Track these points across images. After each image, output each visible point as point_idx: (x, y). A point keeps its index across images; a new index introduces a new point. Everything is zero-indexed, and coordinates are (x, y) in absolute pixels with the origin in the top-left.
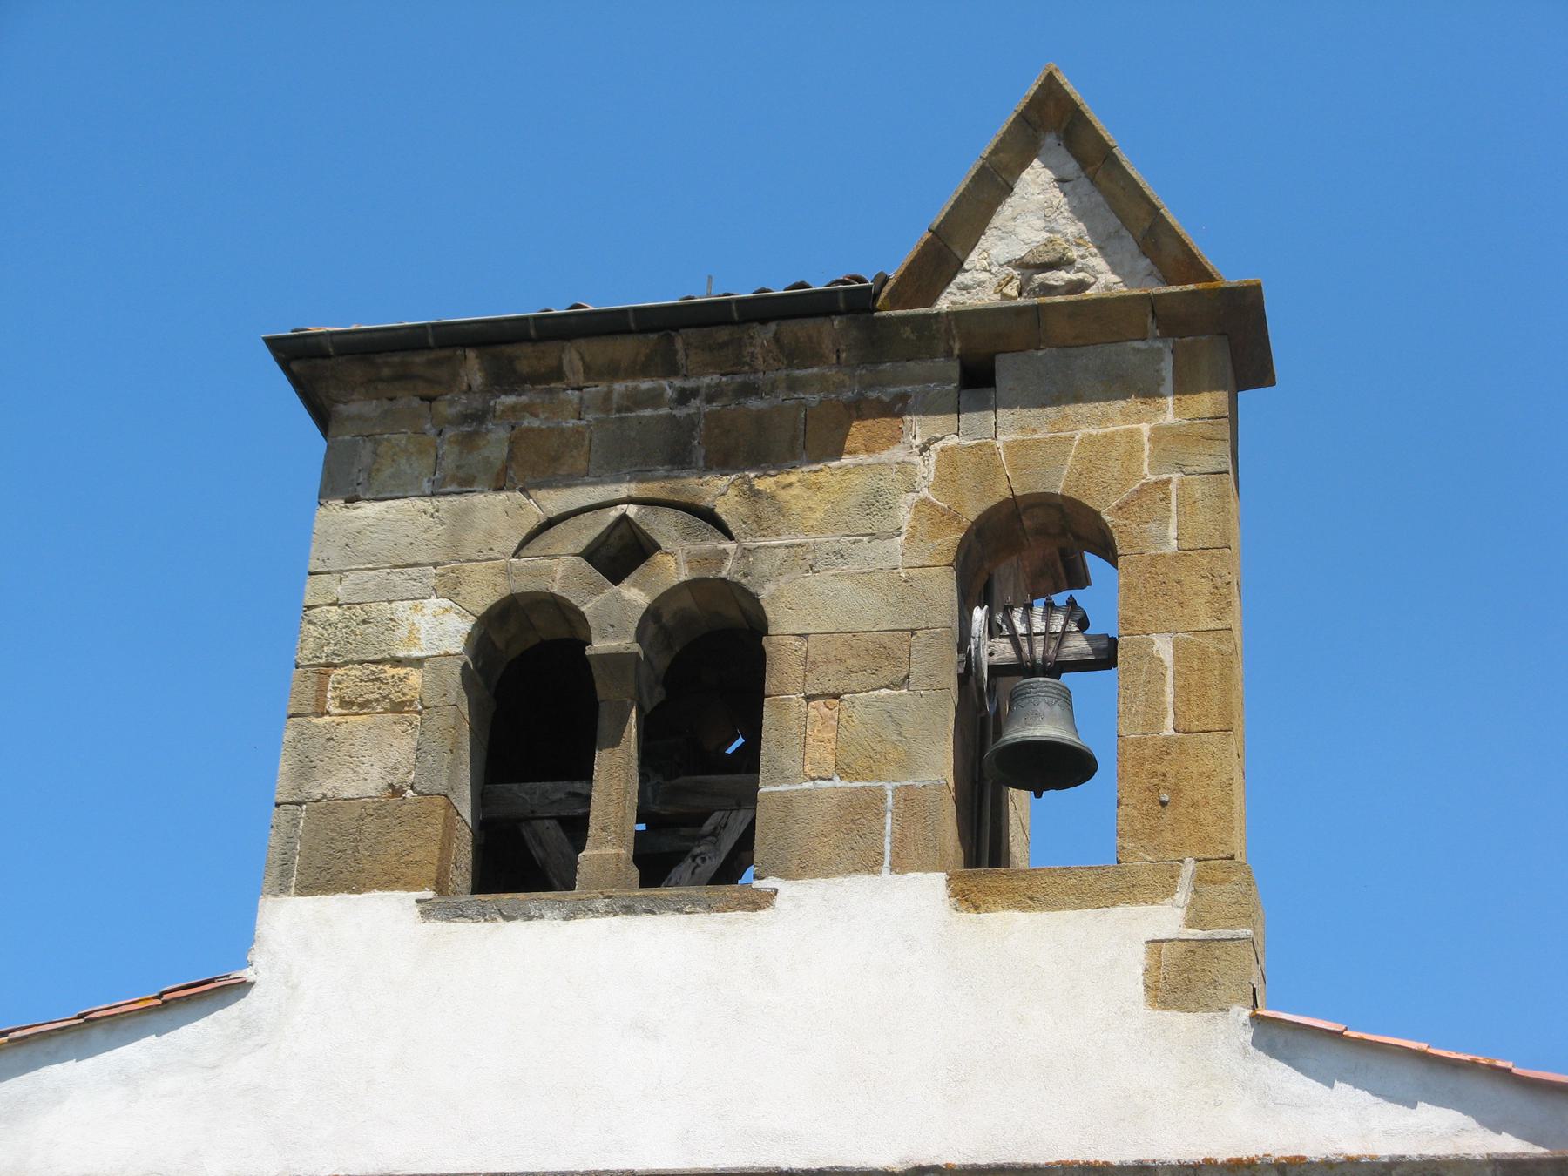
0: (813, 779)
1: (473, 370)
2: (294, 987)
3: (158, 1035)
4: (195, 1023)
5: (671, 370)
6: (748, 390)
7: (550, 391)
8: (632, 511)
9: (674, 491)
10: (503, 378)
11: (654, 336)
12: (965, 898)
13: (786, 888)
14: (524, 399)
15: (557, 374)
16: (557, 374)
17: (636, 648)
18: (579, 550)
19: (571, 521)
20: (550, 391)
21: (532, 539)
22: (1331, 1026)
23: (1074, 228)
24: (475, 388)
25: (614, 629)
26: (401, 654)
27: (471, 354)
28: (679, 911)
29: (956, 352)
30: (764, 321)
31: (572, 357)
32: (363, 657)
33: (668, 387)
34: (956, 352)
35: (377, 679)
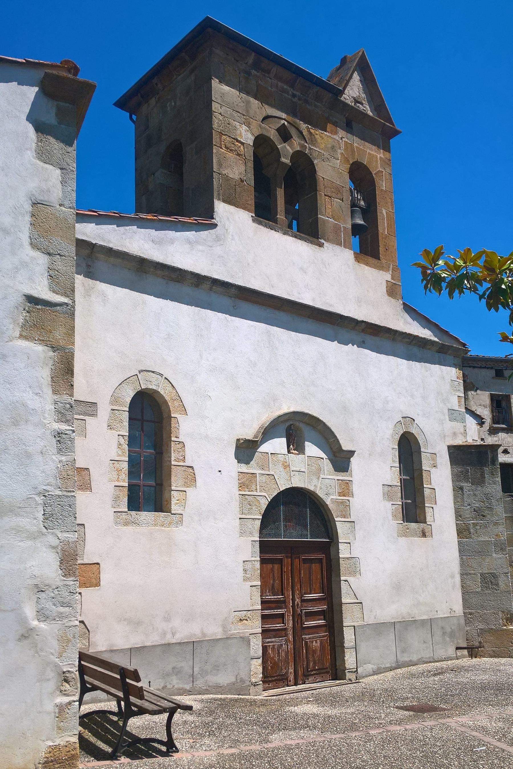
0: (328, 217)
1: (251, 58)
2: (227, 230)
3: (196, 232)
4: (205, 232)
5: (292, 86)
6: (306, 101)
7: (264, 75)
8: (286, 123)
9: (294, 122)
10: (256, 65)
11: (294, 75)
12: (357, 259)
13: (326, 244)
14: (258, 74)
15: (269, 72)
16: (269, 72)
17: (290, 164)
18: (276, 129)
19: (273, 119)
20: (264, 75)
21: (265, 119)
22: (103, 686)
23: (364, 95)
24: (248, 64)
25: (286, 157)
26: (239, 139)
27: (253, 54)
28: (305, 241)
29: (346, 116)
30: (317, 86)
31: (275, 69)
32: (230, 135)
33: (291, 91)
34: (346, 116)
35: (234, 144)
